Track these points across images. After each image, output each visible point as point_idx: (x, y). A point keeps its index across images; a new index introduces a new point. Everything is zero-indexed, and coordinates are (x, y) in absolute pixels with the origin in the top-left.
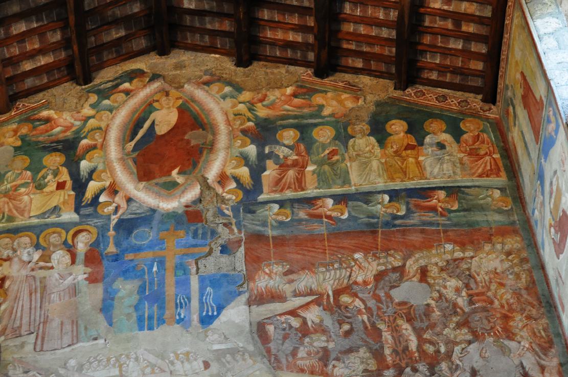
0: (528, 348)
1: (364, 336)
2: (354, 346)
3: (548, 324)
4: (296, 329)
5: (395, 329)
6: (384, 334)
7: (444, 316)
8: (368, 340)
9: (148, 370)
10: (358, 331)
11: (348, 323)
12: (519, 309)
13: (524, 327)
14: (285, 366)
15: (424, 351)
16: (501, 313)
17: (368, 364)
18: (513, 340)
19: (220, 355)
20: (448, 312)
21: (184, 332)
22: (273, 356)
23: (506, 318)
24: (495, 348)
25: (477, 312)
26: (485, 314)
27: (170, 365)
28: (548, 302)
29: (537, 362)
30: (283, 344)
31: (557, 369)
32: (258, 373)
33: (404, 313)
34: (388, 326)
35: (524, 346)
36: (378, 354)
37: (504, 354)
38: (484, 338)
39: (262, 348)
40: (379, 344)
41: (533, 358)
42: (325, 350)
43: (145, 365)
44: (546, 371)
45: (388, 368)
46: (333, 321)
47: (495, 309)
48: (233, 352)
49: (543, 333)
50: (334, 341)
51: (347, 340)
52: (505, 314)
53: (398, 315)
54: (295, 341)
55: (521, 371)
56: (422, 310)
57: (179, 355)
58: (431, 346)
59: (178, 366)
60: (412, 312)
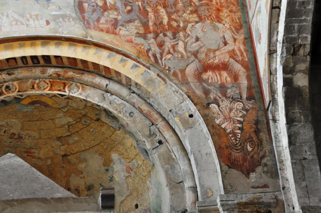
0: (228, 28)
1: (139, 14)
2: (133, 18)
3: (241, 16)
4: (101, 7)
5: (156, 12)
6: (150, 14)
7: (184, 6)
8: (140, 16)
9: (14, 23)
10: (135, 10)
11: (130, 5)
12: (226, 6)
13: (228, 16)
14: (92, 27)
15: (171, 25)
16: (216, 8)
17: (139, 30)
18: (221, 23)
19: (56, 18)
20: (186, 4)
21: (36, 2)
22: (86, 21)
23: (218, 10)
24: (211, 27)
25: (202, 6)
26: (207, 7)
27: (27, 21)
28: (242, 4)
29: (233, 36)
30: (92, 14)
31: (243, 41)
32: (77, 29)
33: (162, 3)
34: (153, 9)
35: (227, 27)
36: (145, 25)
37: (215, 30)
38: (205, 21)
39: (80, 15)
40: (146, 19)
41: (231, 34)
42: (116, 19)
43: (12, 20)
44: (237, 41)
45: (150, 33)
46: (122, 3)
47: (213, 5)
48: (63, 17)
49: (237, 20)
50: (121, 15)
51: (129, 16)
52: (218, 8)
53: (159, 3)
54: (99, 13)
55: (223, 41)
56: (172, 3)
57: (32, 15)
58: (175, 23)
59: (31, 22)
60: (166, 3)
